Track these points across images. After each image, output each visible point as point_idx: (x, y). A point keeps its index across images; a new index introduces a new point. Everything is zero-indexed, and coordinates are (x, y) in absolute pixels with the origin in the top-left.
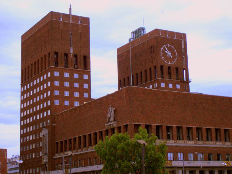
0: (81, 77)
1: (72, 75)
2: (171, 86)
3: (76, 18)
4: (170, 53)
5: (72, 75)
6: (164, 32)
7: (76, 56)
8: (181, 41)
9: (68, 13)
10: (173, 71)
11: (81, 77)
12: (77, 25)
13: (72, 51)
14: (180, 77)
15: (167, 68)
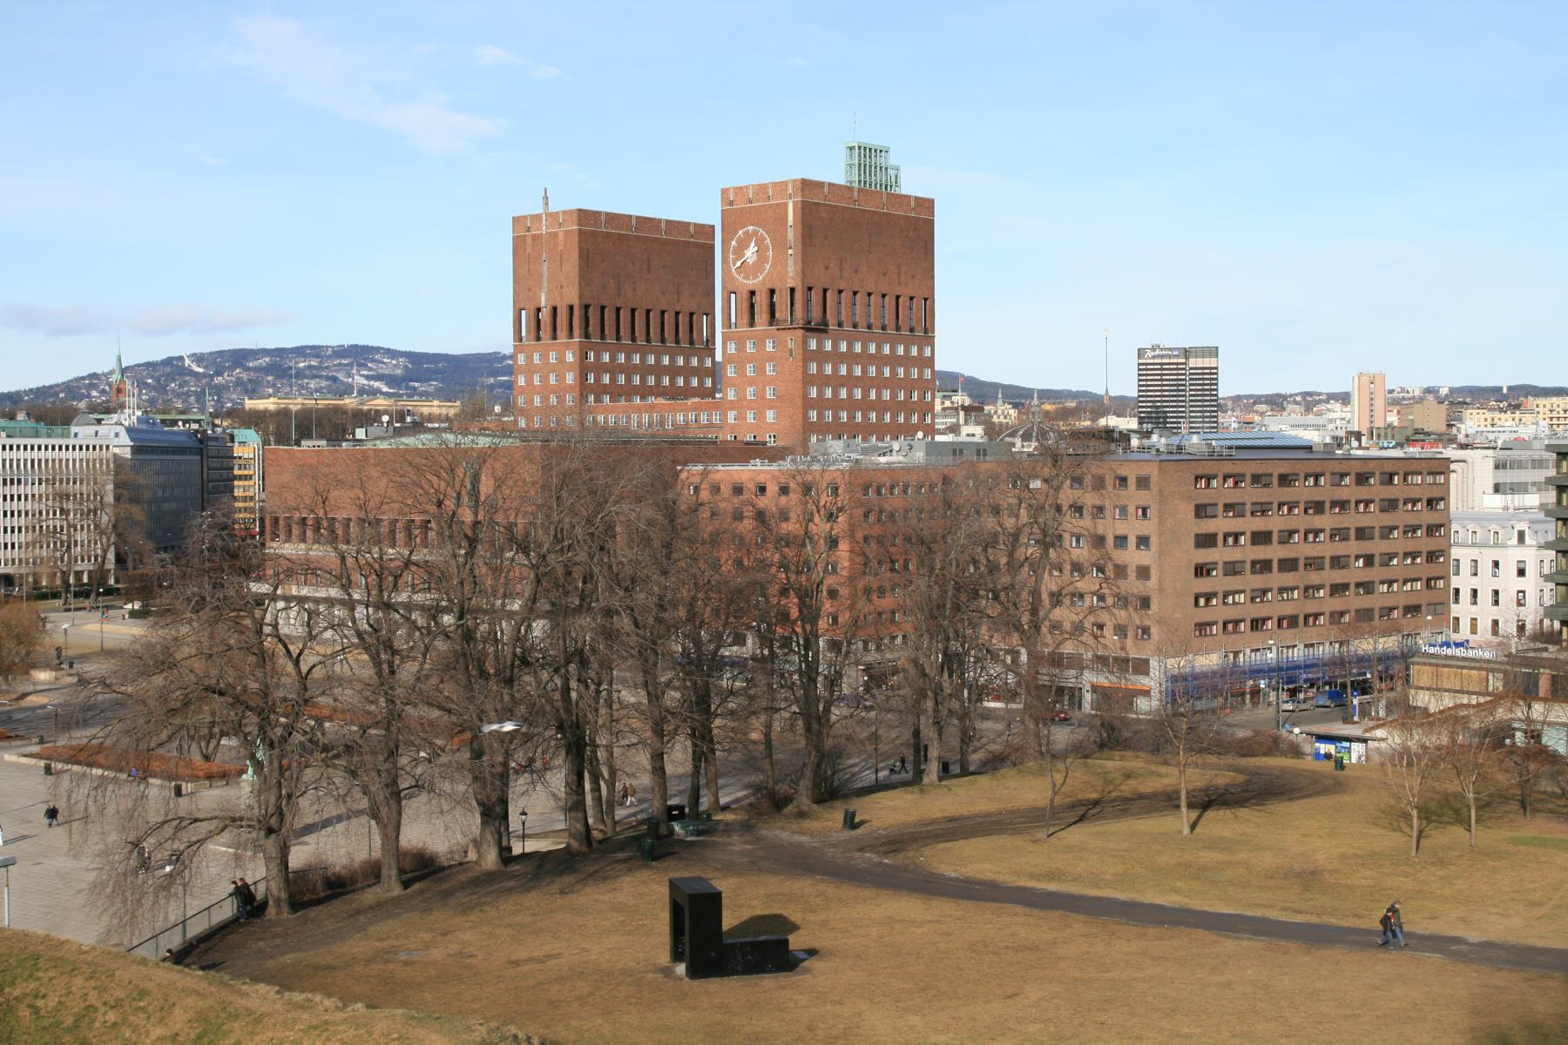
0: (561, 359)
1: (544, 357)
2: (750, 348)
3: (552, 216)
4: (750, 253)
5: (544, 357)
6: (739, 190)
7: (555, 309)
8: (786, 204)
9: (538, 209)
10: (761, 302)
11: (561, 359)
12: (555, 235)
13: (543, 303)
14: (777, 315)
15: (746, 295)
